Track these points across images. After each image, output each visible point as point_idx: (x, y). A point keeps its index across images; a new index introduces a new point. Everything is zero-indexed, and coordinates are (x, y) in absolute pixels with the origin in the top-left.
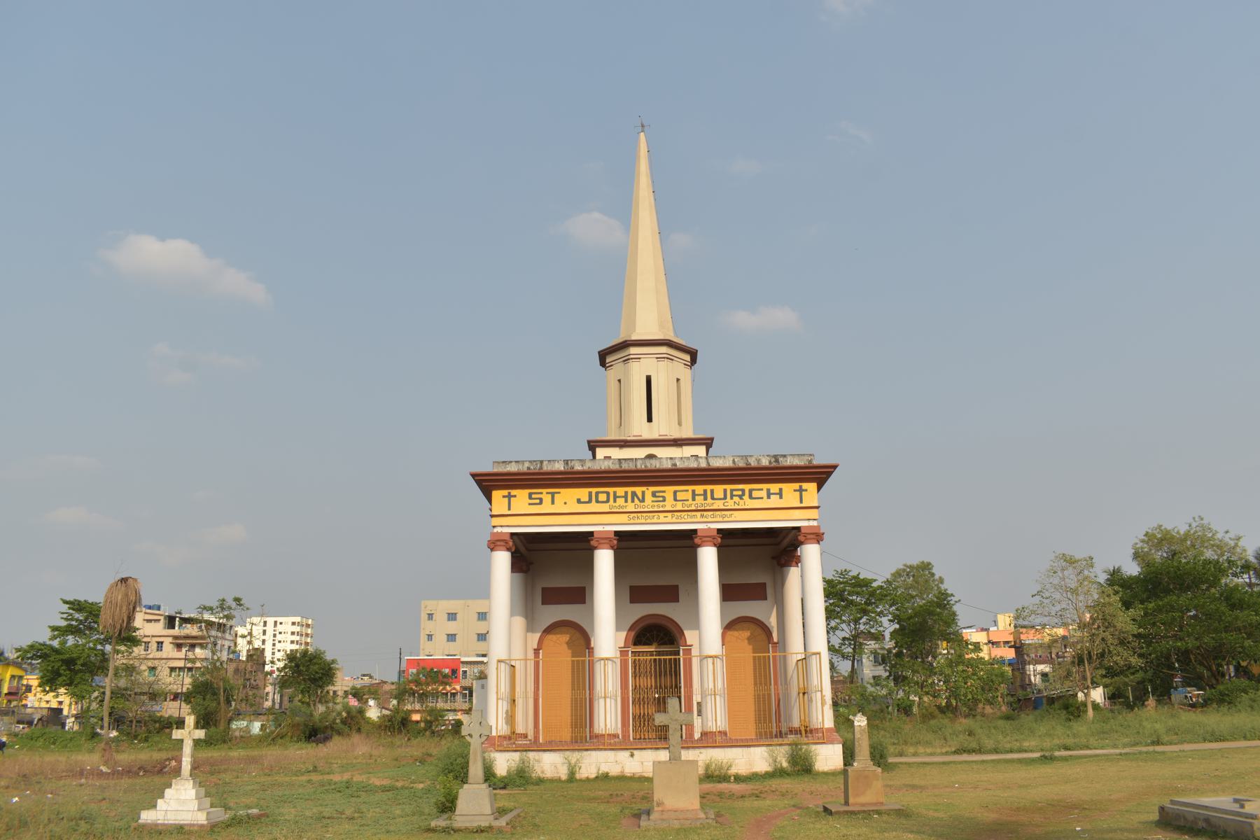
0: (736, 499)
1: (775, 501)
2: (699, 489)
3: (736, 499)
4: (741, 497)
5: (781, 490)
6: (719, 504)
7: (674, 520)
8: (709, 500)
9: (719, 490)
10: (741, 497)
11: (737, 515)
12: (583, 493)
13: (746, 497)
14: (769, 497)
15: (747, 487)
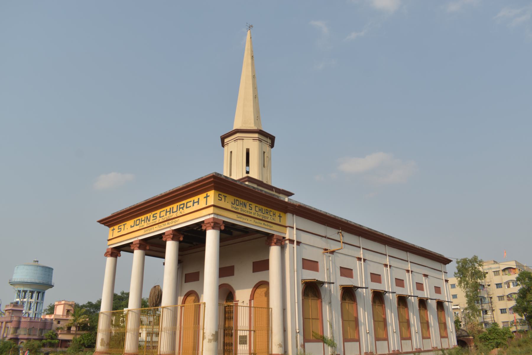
0: (181, 209)
1: (196, 207)
2: (168, 208)
3: (181, 209)
4: (183, 208)
5: (199, 199)
6: (174, 215)
7: (159, 229)
8: (172, 214)
9: (175, 206)
10: (183, 208)
11: (181, 220)
12: (131, 222)
13: (185, 208)
14: (193, 205)
15: (185, 202)
